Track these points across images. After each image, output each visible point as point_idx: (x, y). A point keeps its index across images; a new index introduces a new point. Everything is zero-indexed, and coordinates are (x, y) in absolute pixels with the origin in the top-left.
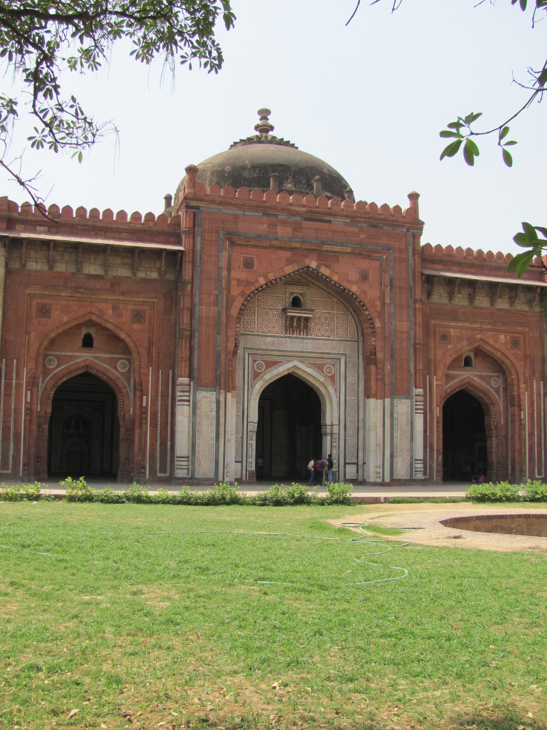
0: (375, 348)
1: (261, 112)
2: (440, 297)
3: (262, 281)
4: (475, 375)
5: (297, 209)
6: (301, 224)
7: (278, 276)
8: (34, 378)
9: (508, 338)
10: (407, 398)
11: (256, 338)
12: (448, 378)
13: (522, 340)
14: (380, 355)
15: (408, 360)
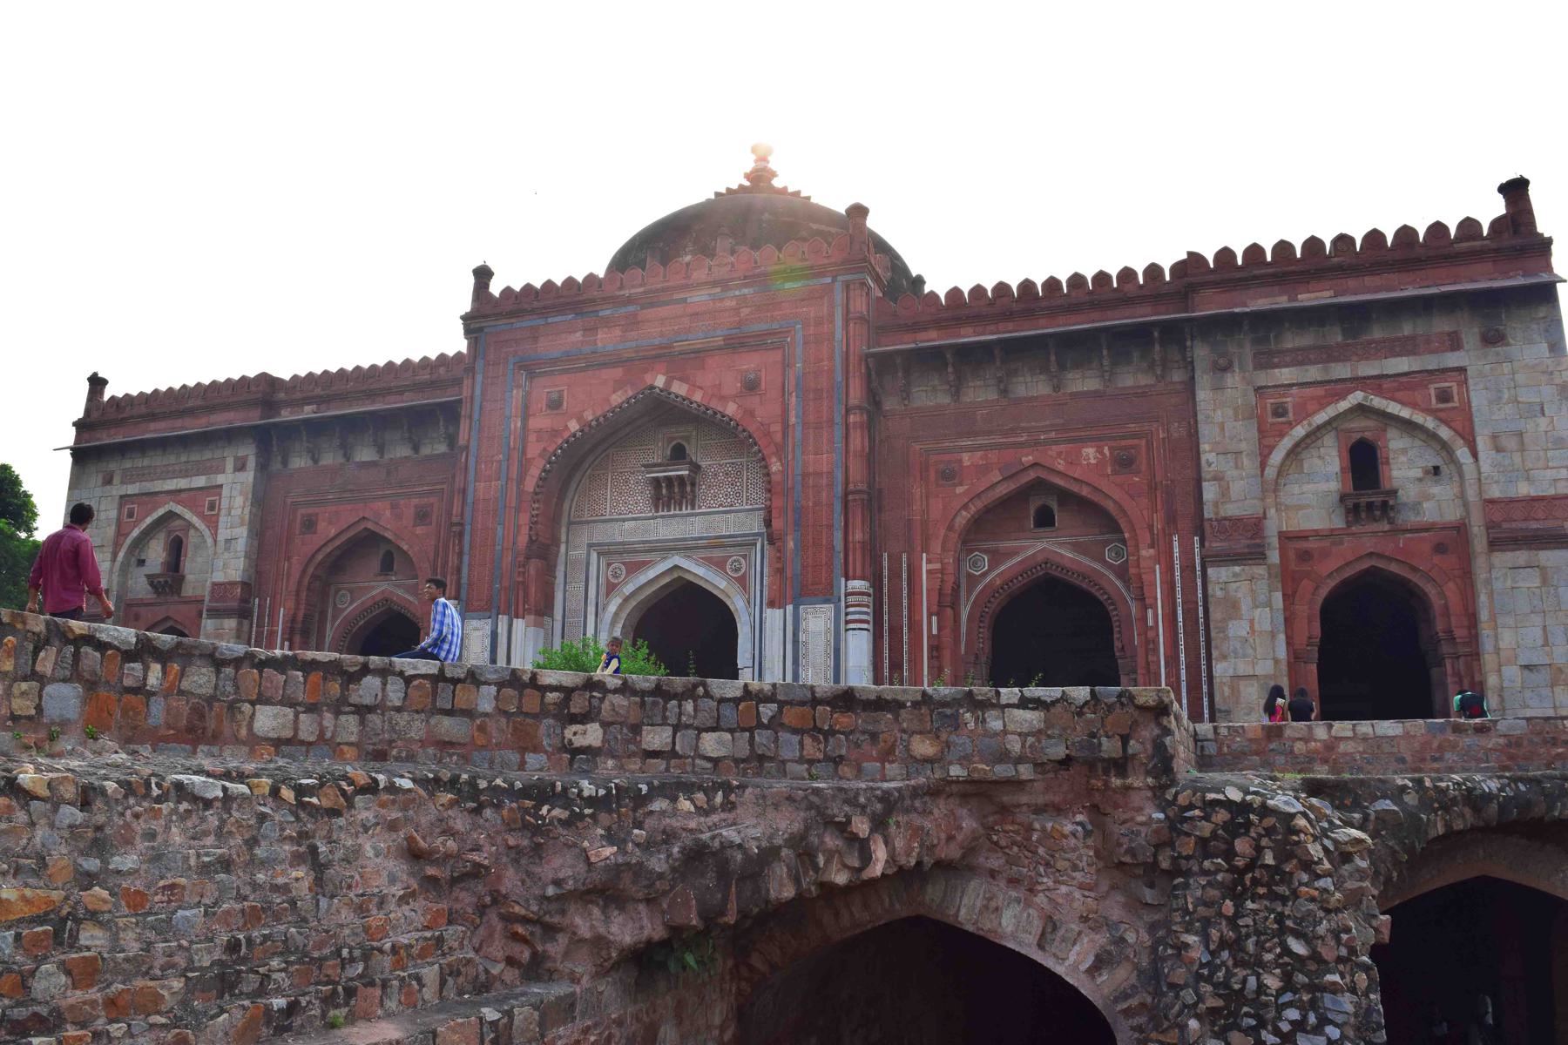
0: (770, 512)
1: (754, 150)
2: (930, 395)
3: (574, 426)
4: (1061, 544)
5: (626, 292)
6: (635, 315)
7: (599, 413)
8: (293, 620)
9: (1106, 450)
10: (826, 601)
11: (609, 525)
12: (997, 557)
13: (1144, 450)
14: (777, 524)
15: (830, 527)
